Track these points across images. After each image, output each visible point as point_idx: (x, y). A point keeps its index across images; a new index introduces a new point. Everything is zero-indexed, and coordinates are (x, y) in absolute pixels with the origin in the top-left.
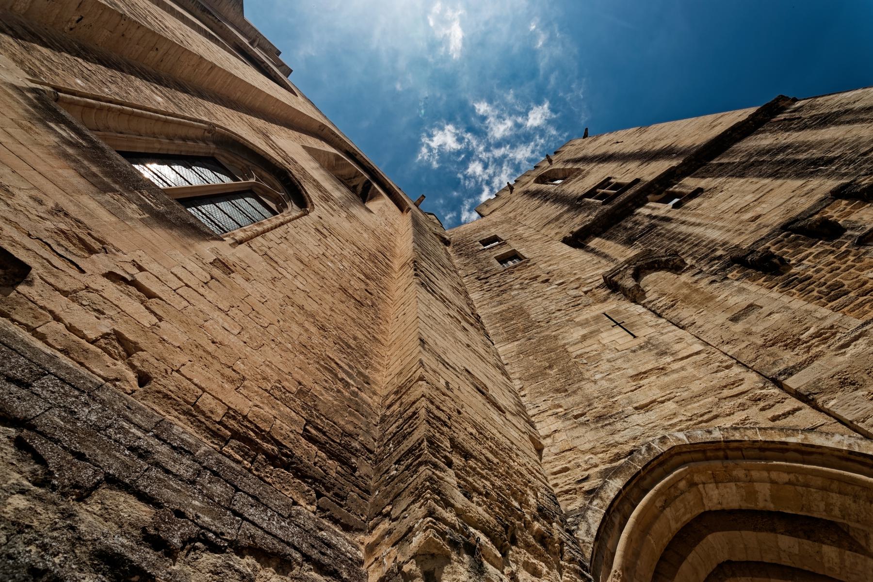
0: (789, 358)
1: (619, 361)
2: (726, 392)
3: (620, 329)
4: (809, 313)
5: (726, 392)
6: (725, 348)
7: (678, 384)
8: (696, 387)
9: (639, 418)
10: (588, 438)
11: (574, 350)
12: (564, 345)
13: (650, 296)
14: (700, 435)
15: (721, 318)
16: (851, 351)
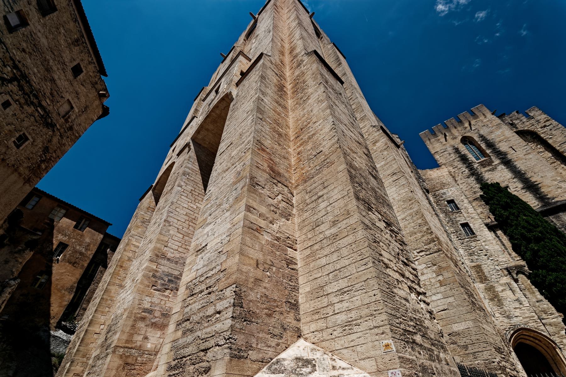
0: (544, 316)
1: (511, 303)
2: (531, 318)
3: (511, 292)
4: (551, 308)
5: (531, 318)
6: (534, 308)
7: (524, 313)
8: (527, 315)
9: (515, 319)
10: (506, 320)
11: (501, 294)
12: (497, 291)
13: (520, 283)
14: (526, 326)
15: (534, 300)
16: (554, 320)
